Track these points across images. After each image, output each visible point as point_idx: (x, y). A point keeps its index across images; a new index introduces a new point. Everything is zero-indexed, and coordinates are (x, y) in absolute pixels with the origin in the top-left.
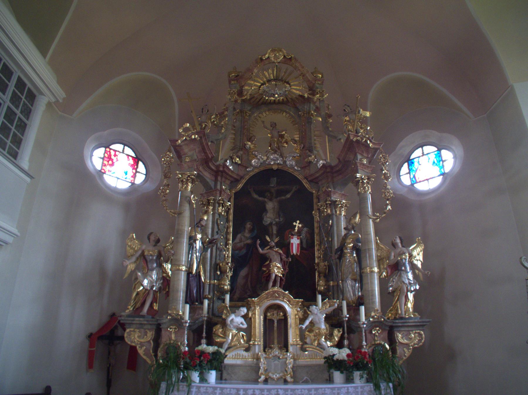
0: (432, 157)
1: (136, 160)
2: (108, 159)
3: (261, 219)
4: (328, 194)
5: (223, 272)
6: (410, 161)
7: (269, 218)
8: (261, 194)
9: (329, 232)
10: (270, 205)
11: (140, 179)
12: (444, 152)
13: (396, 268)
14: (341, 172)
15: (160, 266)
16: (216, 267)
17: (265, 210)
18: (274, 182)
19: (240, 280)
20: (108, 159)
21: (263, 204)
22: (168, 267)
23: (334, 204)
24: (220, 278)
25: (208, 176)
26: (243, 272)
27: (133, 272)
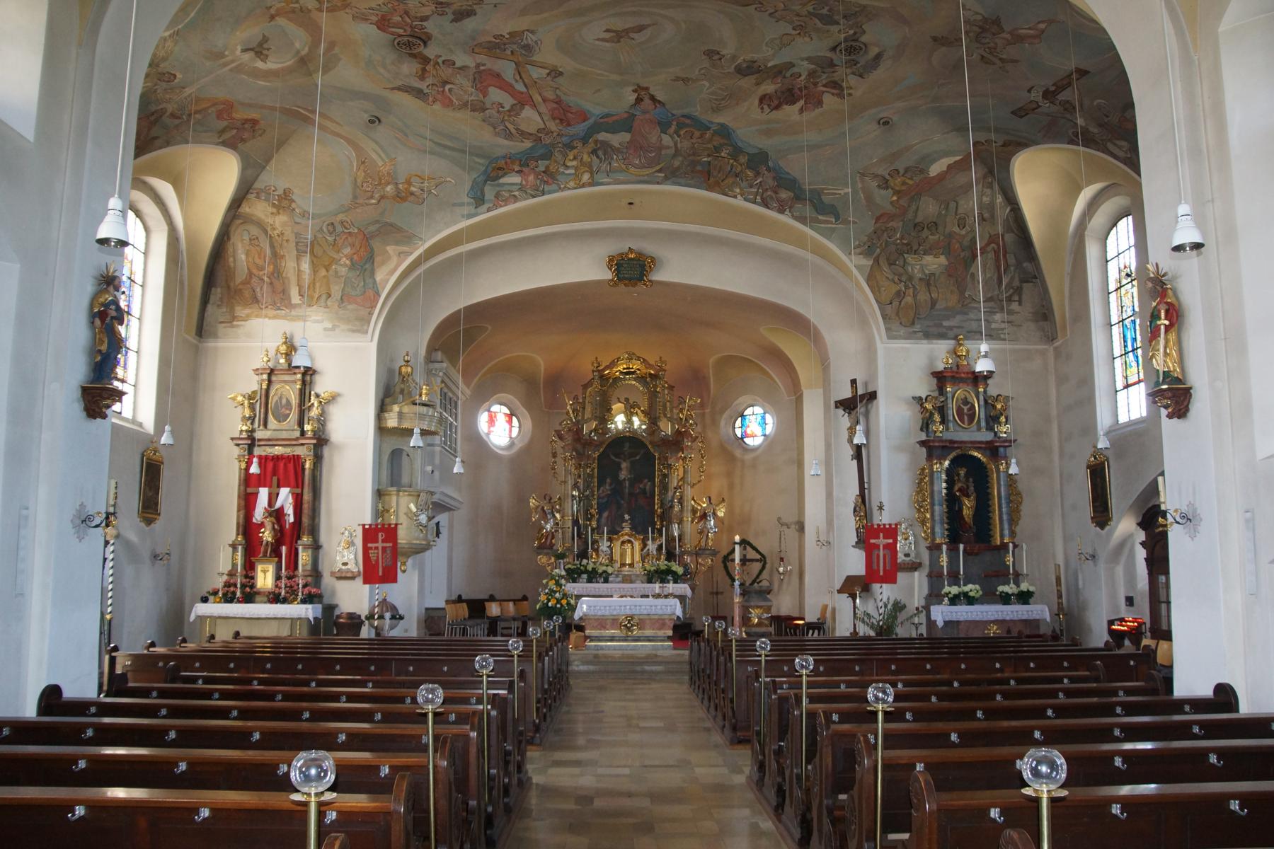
0: (759, 418)
1: (510, 416)
2: (492, 421)
3: (618, 476)
4: (666, 459)
5: (593, 516)
6: (742, 416)
7: (623, 475)
8: (616, 456)
9: (665, 488)
10: (624, 465)
11: (515, 432)
12: (768, 416)
13: (704, 516)
14: (675, 443)
15: (554, 516)
16: (587, 512)
17: (621, 469)
18: (627, 445)
19: (603, 520)
20: (492, 421)
21: (619, 464)
22: (558, 516)
23: (670, 467)
24: (590, 520)
25: (579, 447)
26: (605, 514)
27: (538, 520)
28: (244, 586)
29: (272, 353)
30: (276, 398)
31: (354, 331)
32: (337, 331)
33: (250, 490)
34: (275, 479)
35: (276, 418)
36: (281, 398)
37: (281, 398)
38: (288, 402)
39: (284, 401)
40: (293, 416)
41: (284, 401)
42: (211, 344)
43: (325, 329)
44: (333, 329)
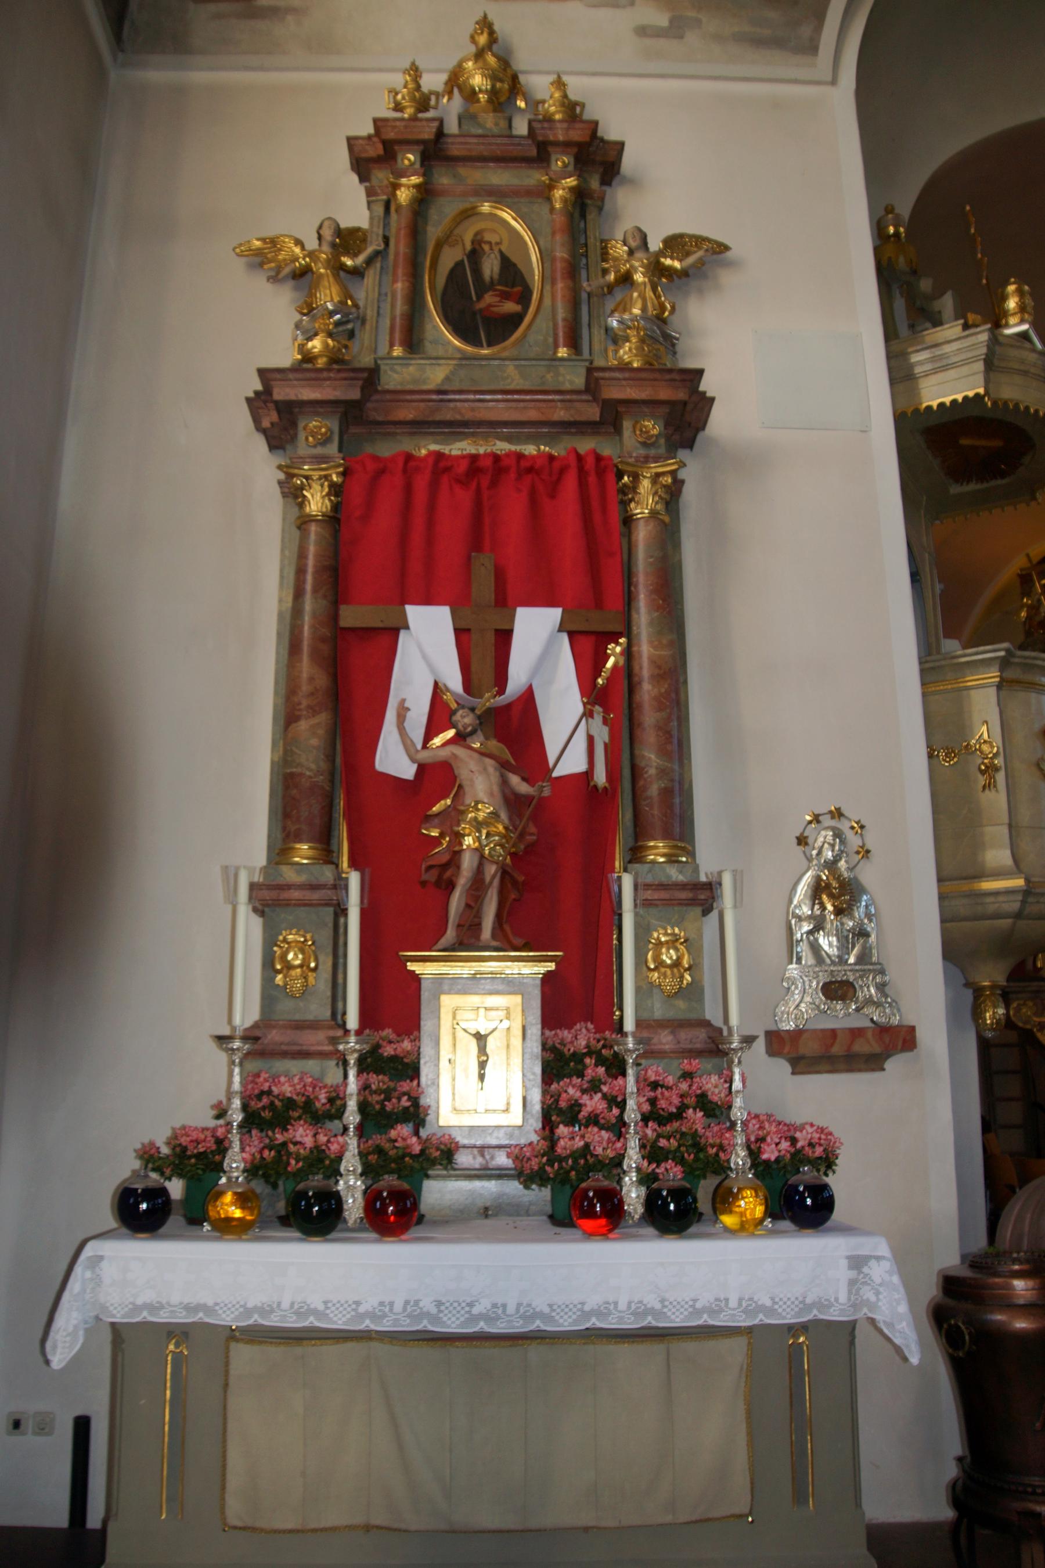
28: (375, 1118)
29: (433, 81)
30: (449, 258)
31: (759, 42)
32: (692, 38)
33: (351, 616)
34: (483, 567)
35: (464, 329)
36: (475, 255)
37: (475, 255)
38: (512, 276)
39: (490, 267)
40: (549, 306)
41: (490, 267)
42: (157, 75)
43: (642, 31)
44: (676, 29)
